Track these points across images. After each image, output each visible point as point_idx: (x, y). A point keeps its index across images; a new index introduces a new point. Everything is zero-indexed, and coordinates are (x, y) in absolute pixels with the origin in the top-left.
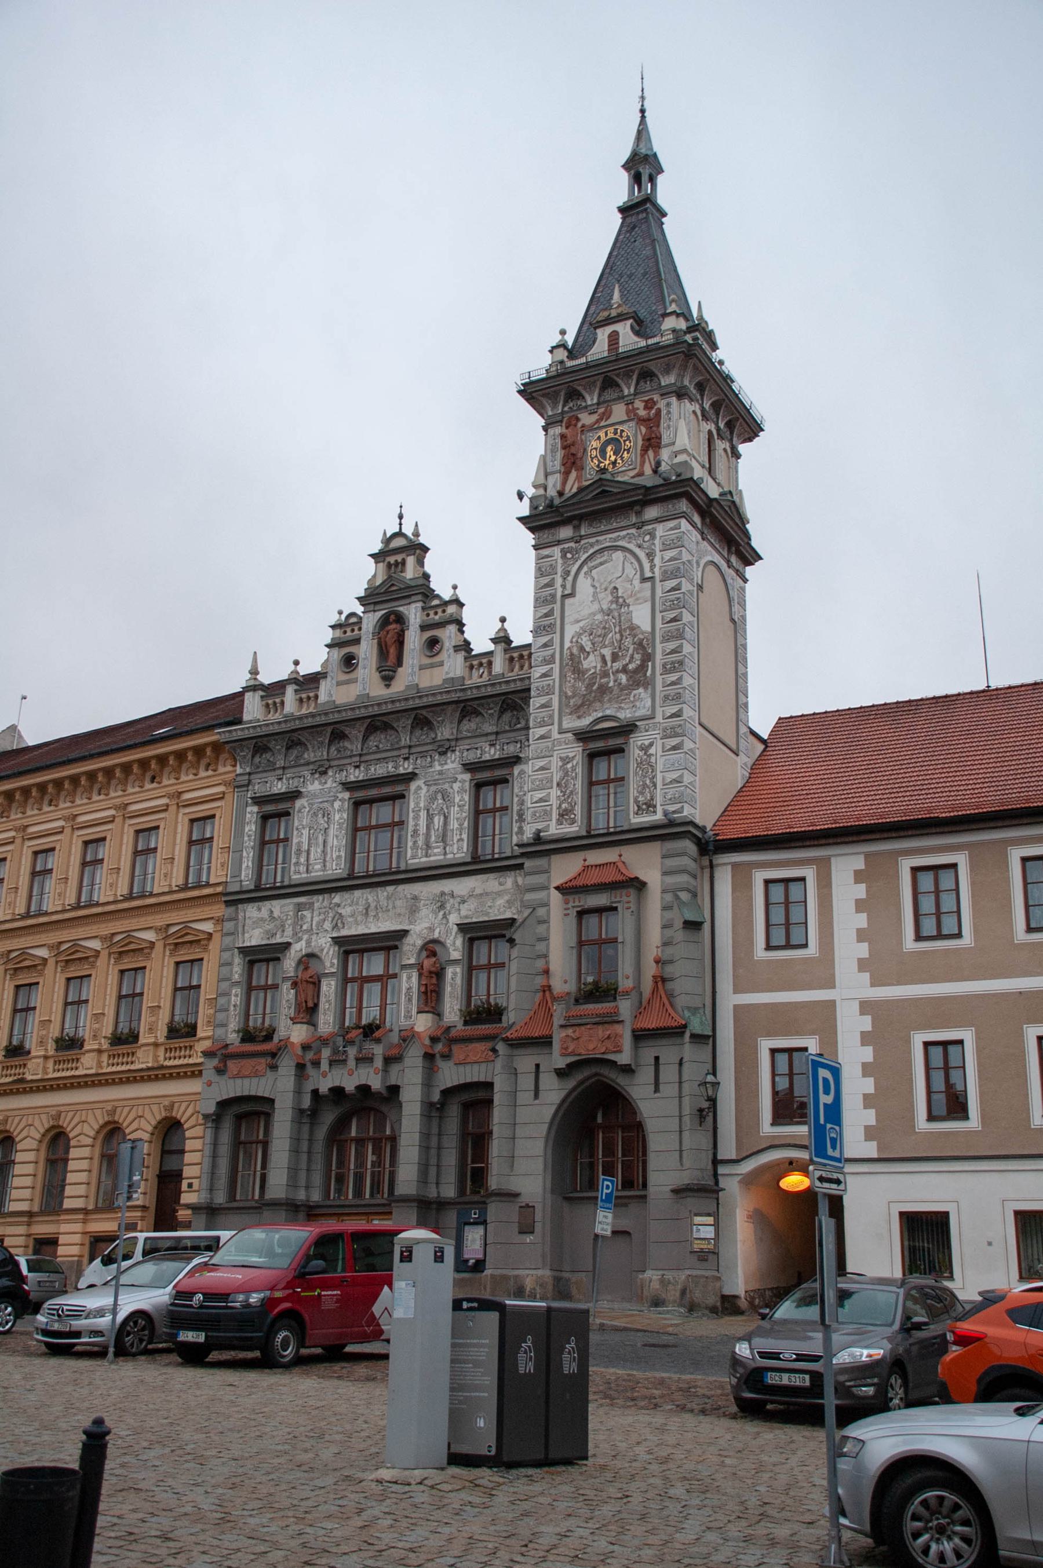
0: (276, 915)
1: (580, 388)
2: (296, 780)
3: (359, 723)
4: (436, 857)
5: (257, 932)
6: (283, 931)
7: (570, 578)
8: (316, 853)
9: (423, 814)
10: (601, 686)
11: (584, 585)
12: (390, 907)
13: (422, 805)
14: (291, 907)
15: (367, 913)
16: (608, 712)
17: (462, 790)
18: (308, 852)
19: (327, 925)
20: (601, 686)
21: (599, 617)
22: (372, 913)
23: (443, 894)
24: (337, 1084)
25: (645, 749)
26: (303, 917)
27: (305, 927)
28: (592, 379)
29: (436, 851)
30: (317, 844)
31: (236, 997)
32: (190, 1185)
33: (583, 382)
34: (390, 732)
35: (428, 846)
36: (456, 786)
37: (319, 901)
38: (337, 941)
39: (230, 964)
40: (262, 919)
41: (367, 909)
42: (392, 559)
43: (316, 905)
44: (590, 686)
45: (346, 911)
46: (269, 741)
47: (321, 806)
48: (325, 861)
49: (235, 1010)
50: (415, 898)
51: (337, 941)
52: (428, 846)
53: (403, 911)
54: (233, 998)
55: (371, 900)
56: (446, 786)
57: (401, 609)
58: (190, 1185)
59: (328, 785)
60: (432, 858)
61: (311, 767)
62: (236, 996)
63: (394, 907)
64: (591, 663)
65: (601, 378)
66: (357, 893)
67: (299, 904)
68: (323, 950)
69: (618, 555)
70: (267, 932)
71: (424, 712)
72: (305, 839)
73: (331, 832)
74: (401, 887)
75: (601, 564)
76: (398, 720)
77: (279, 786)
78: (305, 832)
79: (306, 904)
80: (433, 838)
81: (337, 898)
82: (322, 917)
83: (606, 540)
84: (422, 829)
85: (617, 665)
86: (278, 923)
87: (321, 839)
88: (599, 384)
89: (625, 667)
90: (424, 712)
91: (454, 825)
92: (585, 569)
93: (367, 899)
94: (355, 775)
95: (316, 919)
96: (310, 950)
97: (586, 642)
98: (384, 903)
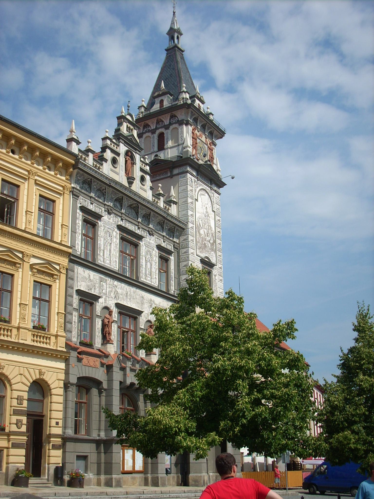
0: (92, 278)
1: (199, 119)
2: (98, 209)
3: (132, 201)
4: (148, 282)
5: (83, 284)
6: (95, 289)
7: (197, 193)
8: (107, 253)
9: (144, 258)
10: (205, 244)
11: (199, 199)
12: (135, 297)
13: (144, 254)
14: (98, 278)
15: (127, 296)
16: (207, 256)
17: (155, 256)
18: (104, 251)
19: (112, 294)
20: (205, 244)
21: (203, 215)
22: (129, 297)
23: (151, 300)
24: (133, 381)
25: (215, 276)
26: (103, 286)
27: (104, 291)
28: (203, 120)
29: (149, 278)
30: (107, 249)
31: (75, 317)
32: (57, 423)
33: (201, 119)
34: (133, 210)
35: (146, 276)
36: (154, 252)
37: (109, 280)
38: (118, 305)
39: (72, 297)
40: (85, 278)
41: (127, 294)
42: (129, 125)
43: (108, 282)
44: (202, 241)
45: (120, 291)
46: (94, 182)
47: (109, 230)
48: (110, 260)
49: (75, 324)
50: (143, 297)
51: (118, 305)
52: (146, 276)
53: (139, 301)
54: (74, 317)
55: (128, 290)
56: (151, 250)
57: (134, 153)
58: (57, 423)
59: (111, 221)
60: (148, 282)
61: (106, 207)
62: (75, 316)
63: (136, 298)
64: (202, 232)
65: (205, 122)
66: (123, 285)
67: (101, 278)
68: (111, 307)
69: (206, 194)
70: (88, 286)
71: (152, 213)
72: (102, 243)
73: (113, 246)
74: (138, 290)
75: (203, 195)
76: (143, 209)
77: (91, 207)
78: (102, 239)
79: (104, 279)
80: (147, 272)
81: (116, 283)
82: (110, 290)
83: (205, 187)
84: (144, 266)
85: (208, 239)
86: (93, 283)
87: (109, 247)
88: (203, 123)
89: (210, 240)
90: (152, 213)
91: (153, 270)
92: (199, 193)
93: (127, 289)
94: (120, 223)
95: (108, 289)
96: (106, 305)
97: (200, 222)
98: (132, 294)
